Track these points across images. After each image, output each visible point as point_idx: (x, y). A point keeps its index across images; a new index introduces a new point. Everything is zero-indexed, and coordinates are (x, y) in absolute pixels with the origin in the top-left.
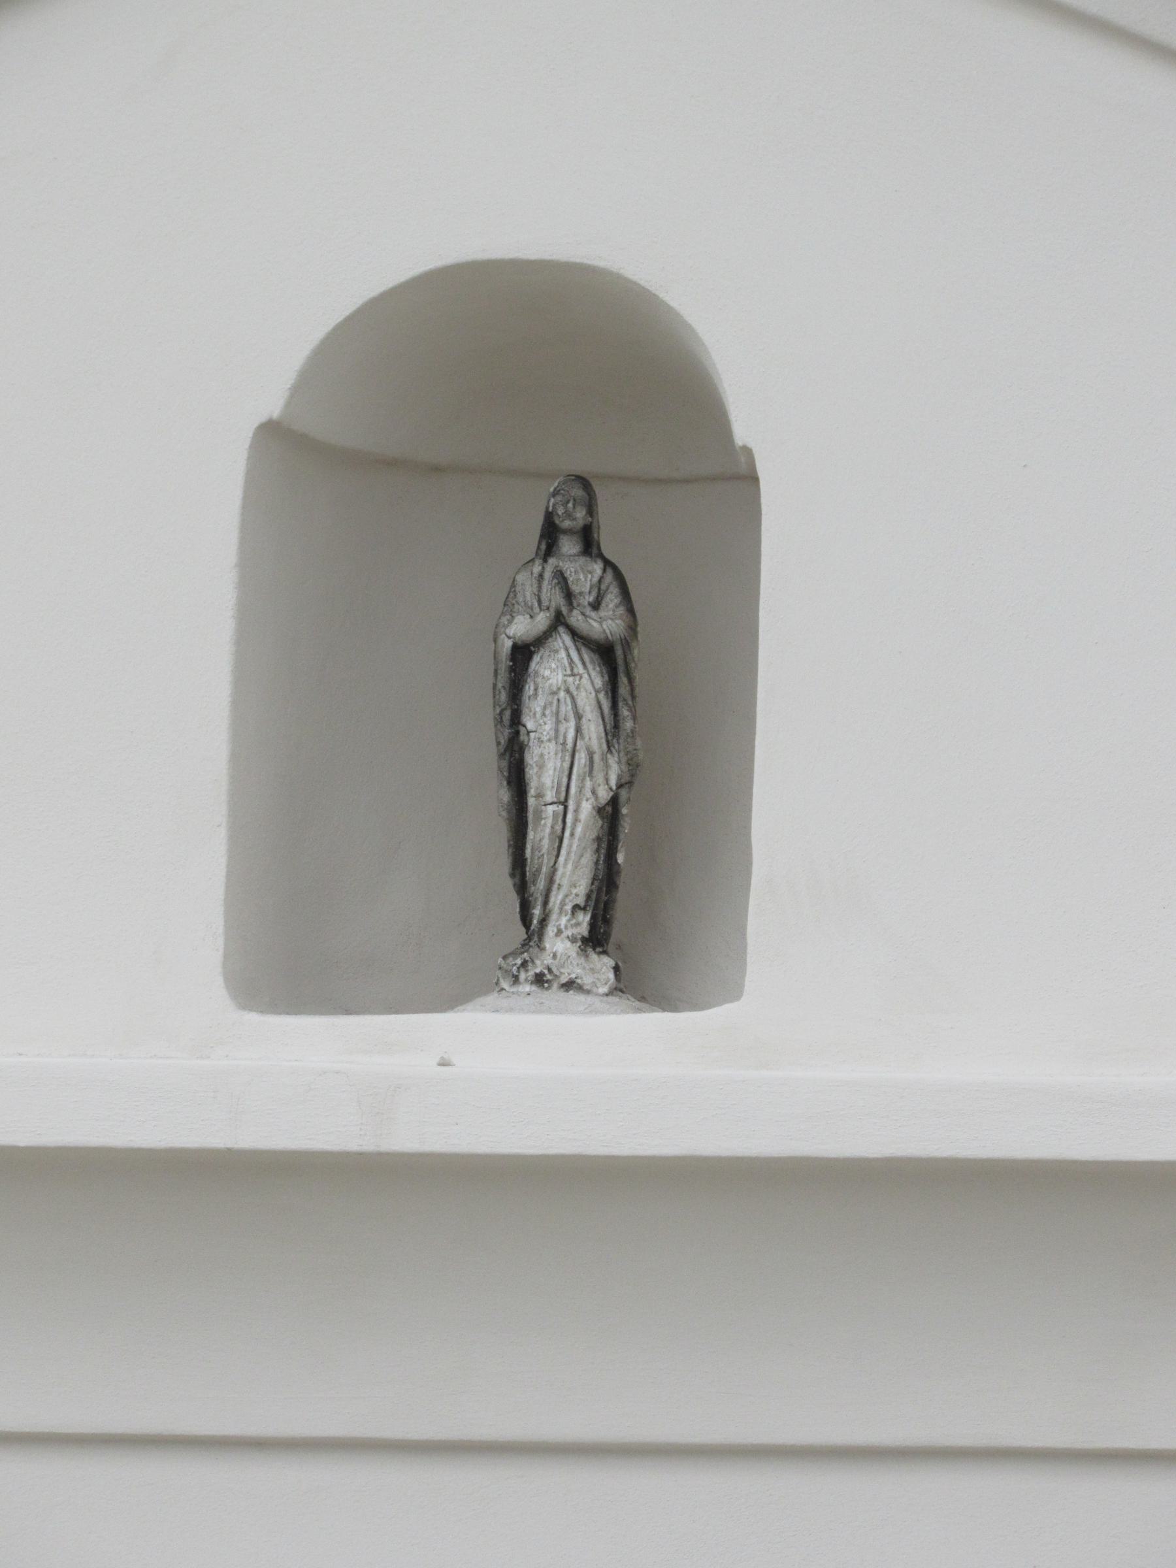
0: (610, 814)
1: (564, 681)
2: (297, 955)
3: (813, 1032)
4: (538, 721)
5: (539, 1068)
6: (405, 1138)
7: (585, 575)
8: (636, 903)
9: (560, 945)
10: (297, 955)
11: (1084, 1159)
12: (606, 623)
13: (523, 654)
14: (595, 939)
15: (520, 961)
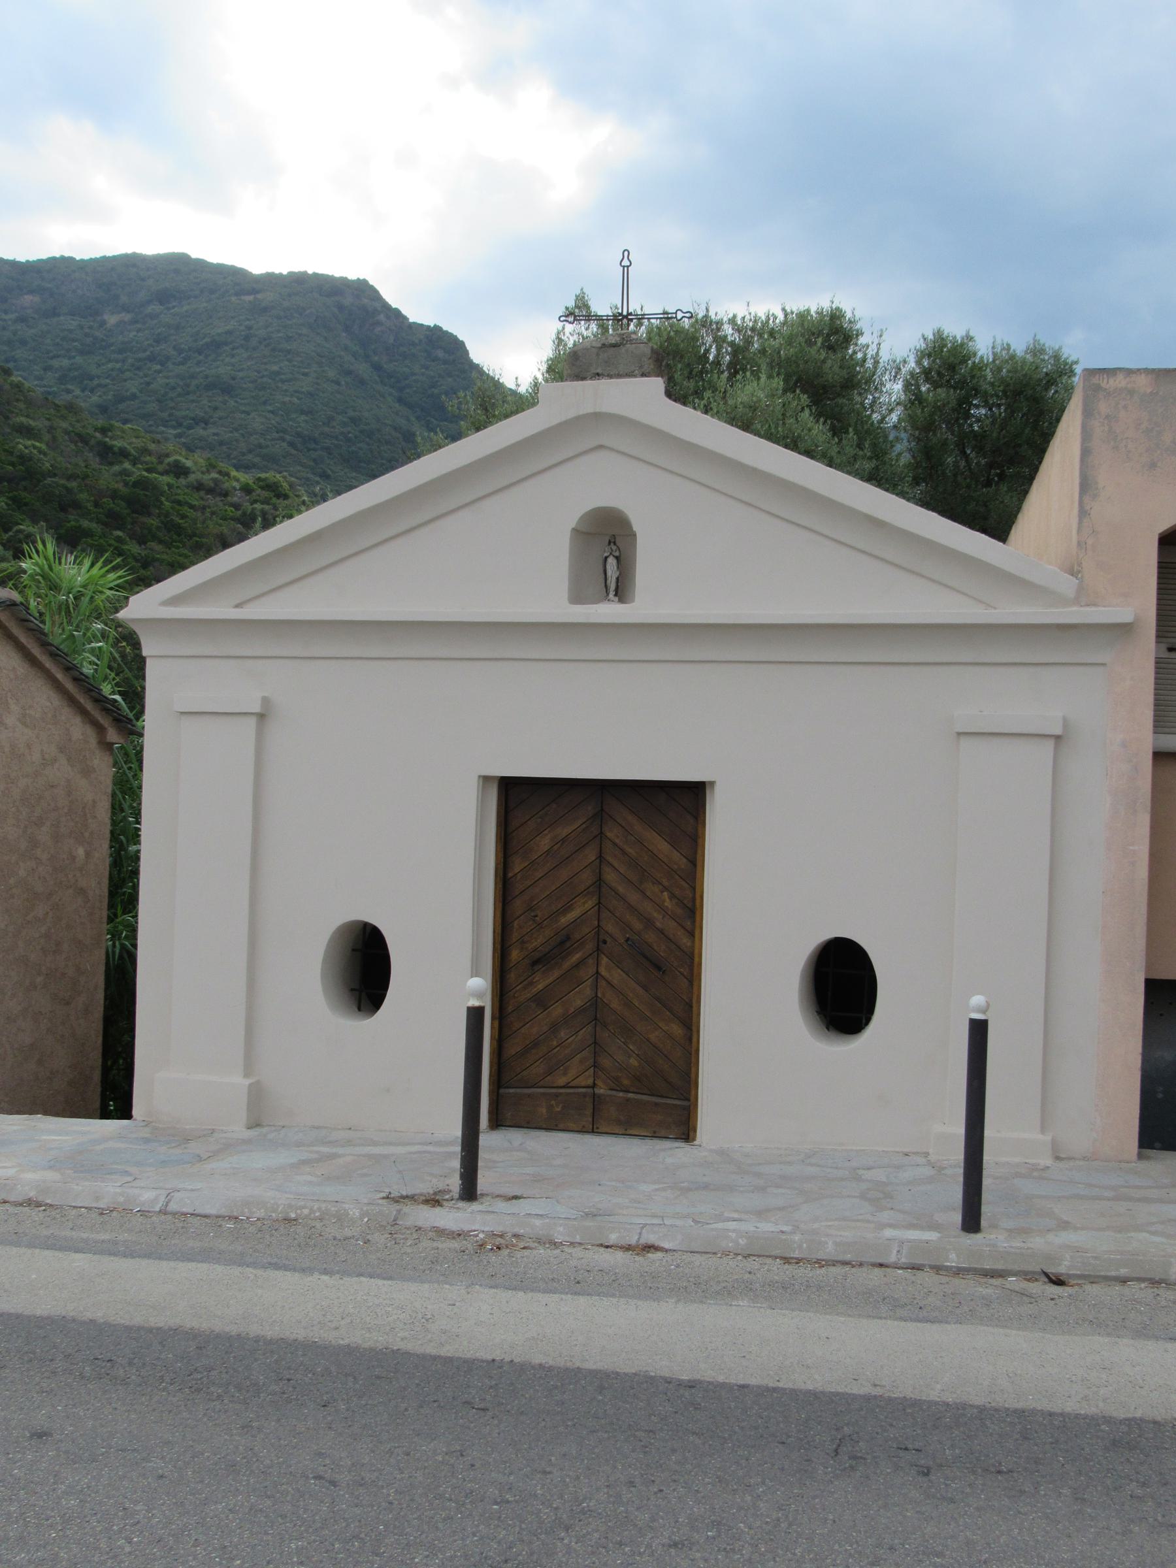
0: (617, 579)
1: (612, 561)
2: (577, 596)
3: (644, 606)
4: (608, 567)
5: (608, 611)
6: (592, 620)
7: (614, 548)
8: (621, 590)
9: (611, 596)
10: (577, 596)
11: (1013, 531)
12: (617, 554)
13: (606, 558)
14: (616, 595)
15: (605, 597)
